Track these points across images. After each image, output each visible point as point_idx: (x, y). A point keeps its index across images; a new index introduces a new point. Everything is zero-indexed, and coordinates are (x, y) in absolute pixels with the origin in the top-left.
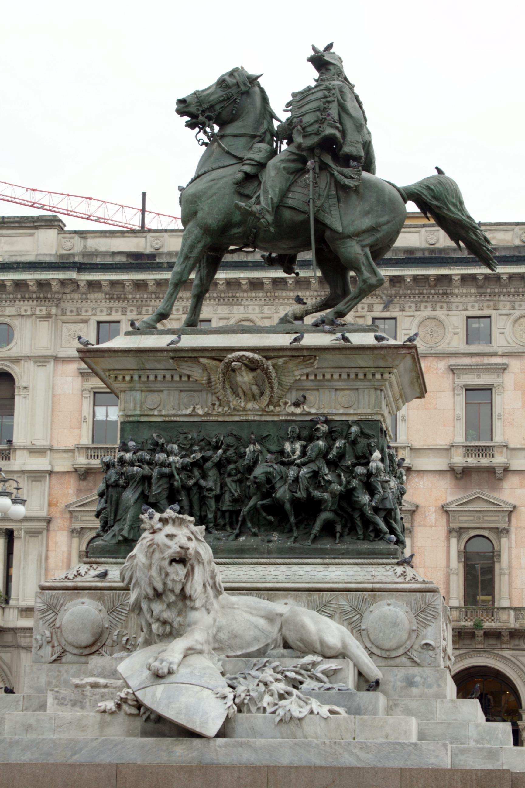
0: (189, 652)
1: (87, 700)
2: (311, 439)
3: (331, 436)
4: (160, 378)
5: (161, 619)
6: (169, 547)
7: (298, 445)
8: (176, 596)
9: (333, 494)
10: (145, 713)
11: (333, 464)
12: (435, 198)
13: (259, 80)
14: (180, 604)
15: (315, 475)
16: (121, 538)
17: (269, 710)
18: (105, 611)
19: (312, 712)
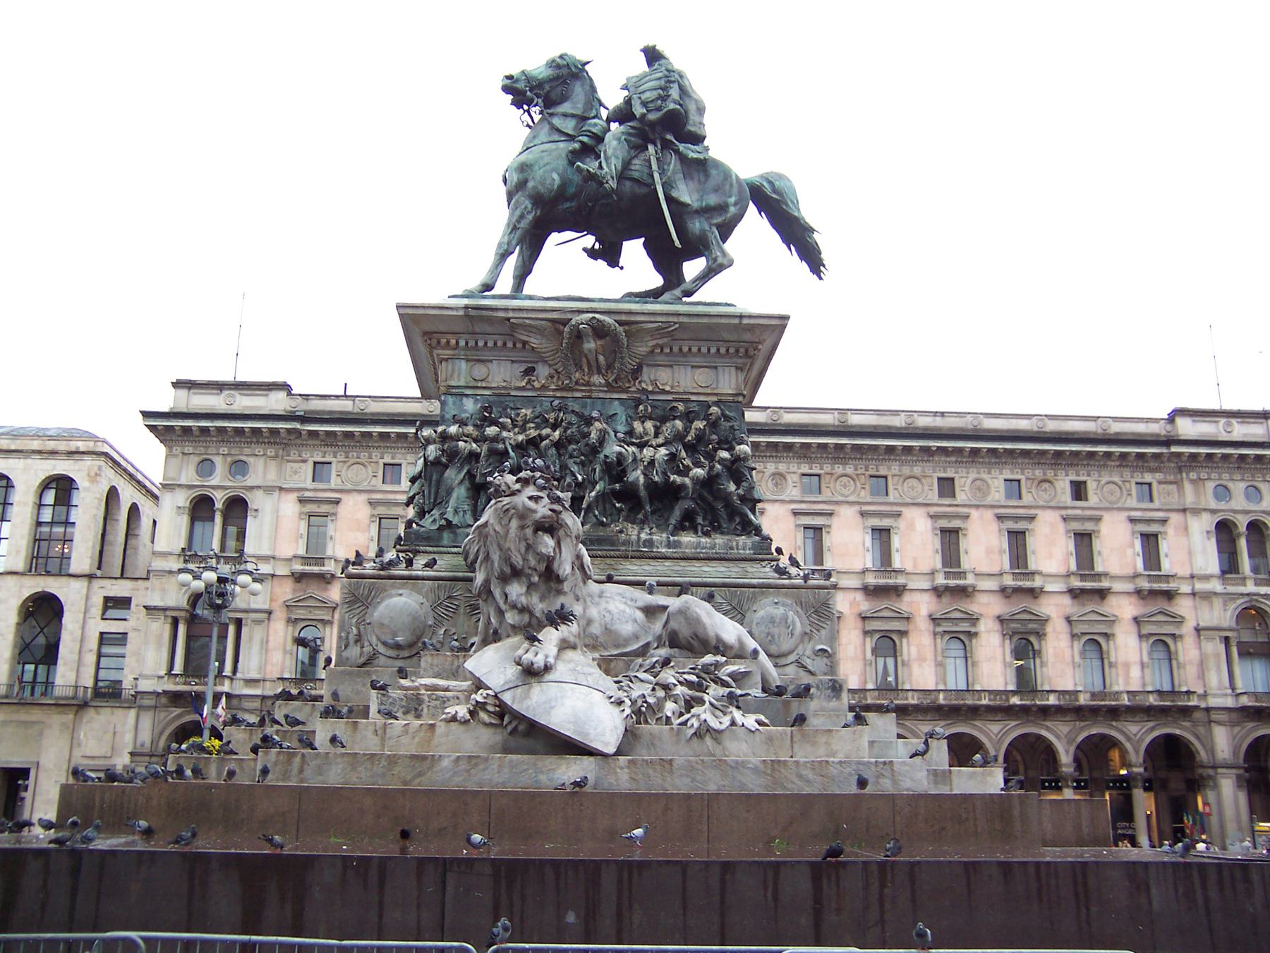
0: (565, 645)
1: (424, 706)
2: (663, 420)
3: (688, 417)
4: (490, 344)
5: (519, 606)
6: (535, 511)
7: (649, 425)
8: (540, 576)
9: (696, 481)
10: (510, 723)
11: (691, 448)
12: (775, 191)
13: (587, 67)
14: (543, 587)
15: (673, 457)
16: (443, 522)
17: (676, 722)
18: (427, 604)
19: (733, 723)
